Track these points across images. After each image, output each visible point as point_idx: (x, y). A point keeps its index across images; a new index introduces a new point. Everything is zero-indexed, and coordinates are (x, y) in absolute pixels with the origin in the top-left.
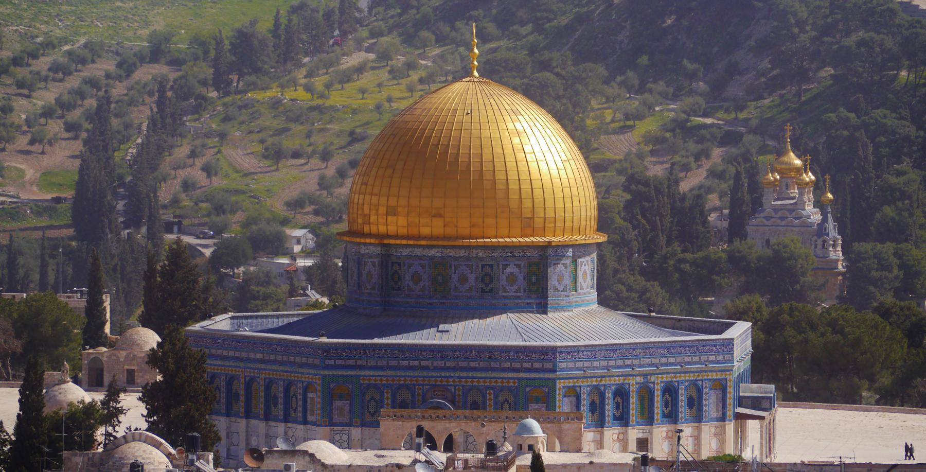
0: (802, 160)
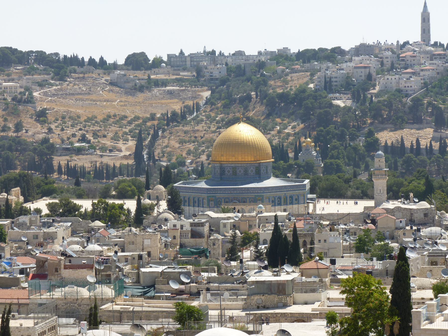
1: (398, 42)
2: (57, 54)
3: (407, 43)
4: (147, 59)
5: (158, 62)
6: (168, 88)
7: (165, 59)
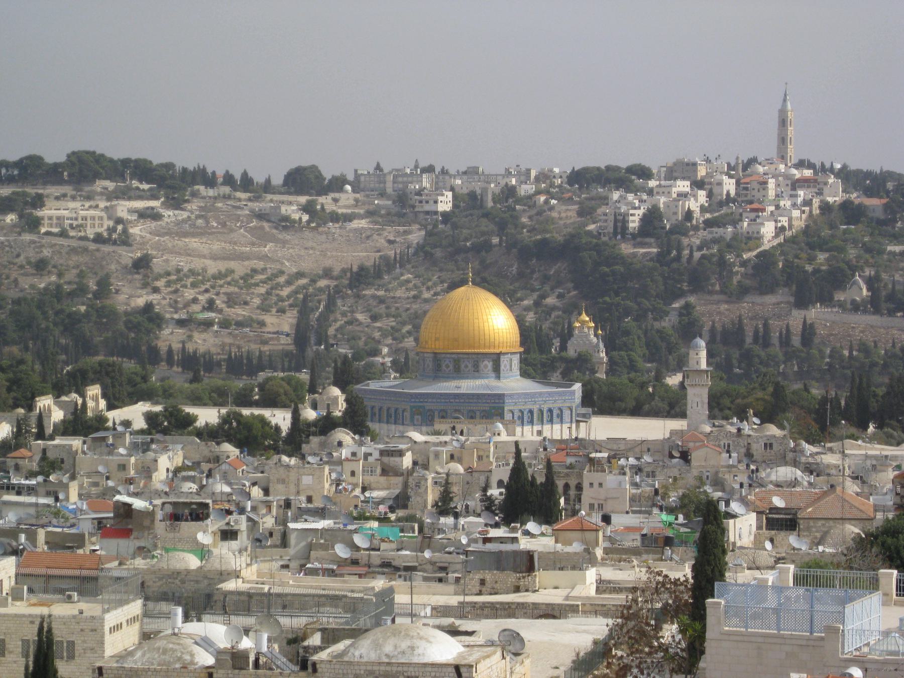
0: (520, 321)
1: (737, 158)
2: (169, 166)
3: (753, 161)
4: (319, 177)
5: (337, 184)
6: (755, 253)
7: (351, 177)
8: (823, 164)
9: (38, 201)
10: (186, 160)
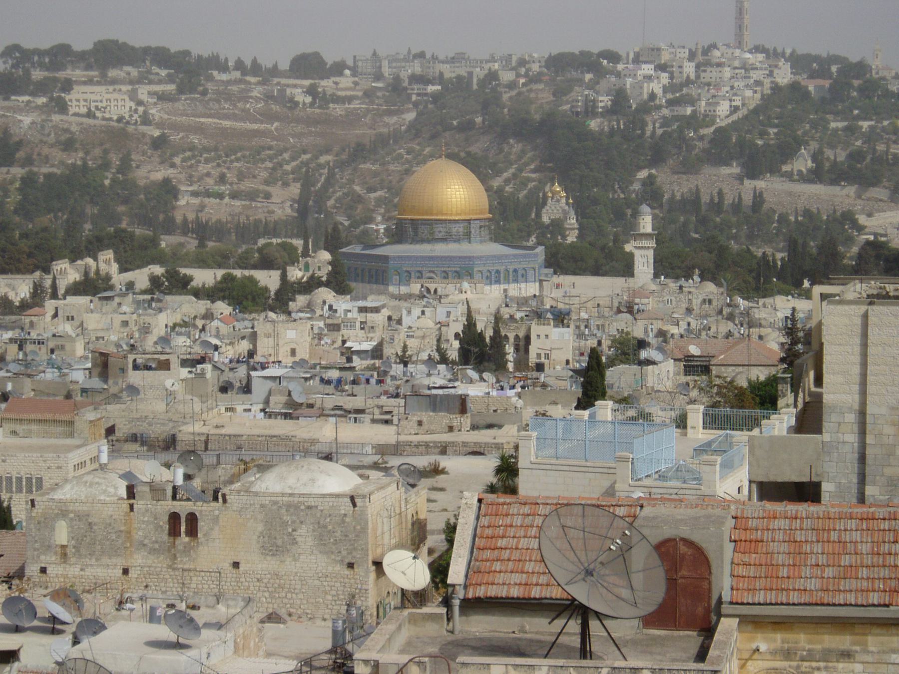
2: (187, 53)
3: (714, 46)
4: (322, 62)
5: (338, 69)
7: (350, 63)
8: (775, 50)
9: (67, 86)
10: (200, 48)
